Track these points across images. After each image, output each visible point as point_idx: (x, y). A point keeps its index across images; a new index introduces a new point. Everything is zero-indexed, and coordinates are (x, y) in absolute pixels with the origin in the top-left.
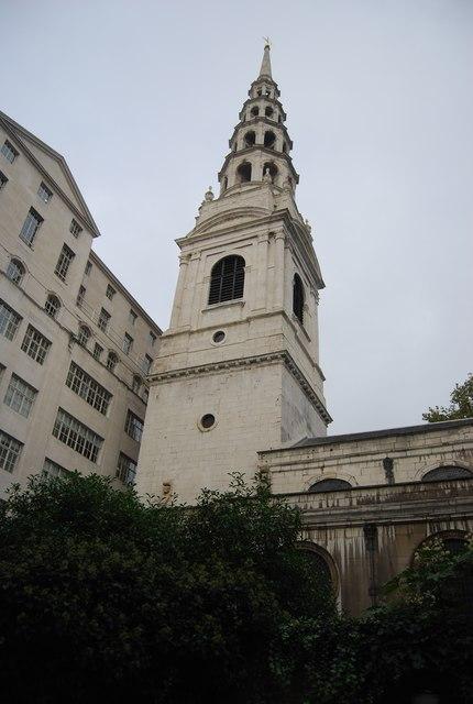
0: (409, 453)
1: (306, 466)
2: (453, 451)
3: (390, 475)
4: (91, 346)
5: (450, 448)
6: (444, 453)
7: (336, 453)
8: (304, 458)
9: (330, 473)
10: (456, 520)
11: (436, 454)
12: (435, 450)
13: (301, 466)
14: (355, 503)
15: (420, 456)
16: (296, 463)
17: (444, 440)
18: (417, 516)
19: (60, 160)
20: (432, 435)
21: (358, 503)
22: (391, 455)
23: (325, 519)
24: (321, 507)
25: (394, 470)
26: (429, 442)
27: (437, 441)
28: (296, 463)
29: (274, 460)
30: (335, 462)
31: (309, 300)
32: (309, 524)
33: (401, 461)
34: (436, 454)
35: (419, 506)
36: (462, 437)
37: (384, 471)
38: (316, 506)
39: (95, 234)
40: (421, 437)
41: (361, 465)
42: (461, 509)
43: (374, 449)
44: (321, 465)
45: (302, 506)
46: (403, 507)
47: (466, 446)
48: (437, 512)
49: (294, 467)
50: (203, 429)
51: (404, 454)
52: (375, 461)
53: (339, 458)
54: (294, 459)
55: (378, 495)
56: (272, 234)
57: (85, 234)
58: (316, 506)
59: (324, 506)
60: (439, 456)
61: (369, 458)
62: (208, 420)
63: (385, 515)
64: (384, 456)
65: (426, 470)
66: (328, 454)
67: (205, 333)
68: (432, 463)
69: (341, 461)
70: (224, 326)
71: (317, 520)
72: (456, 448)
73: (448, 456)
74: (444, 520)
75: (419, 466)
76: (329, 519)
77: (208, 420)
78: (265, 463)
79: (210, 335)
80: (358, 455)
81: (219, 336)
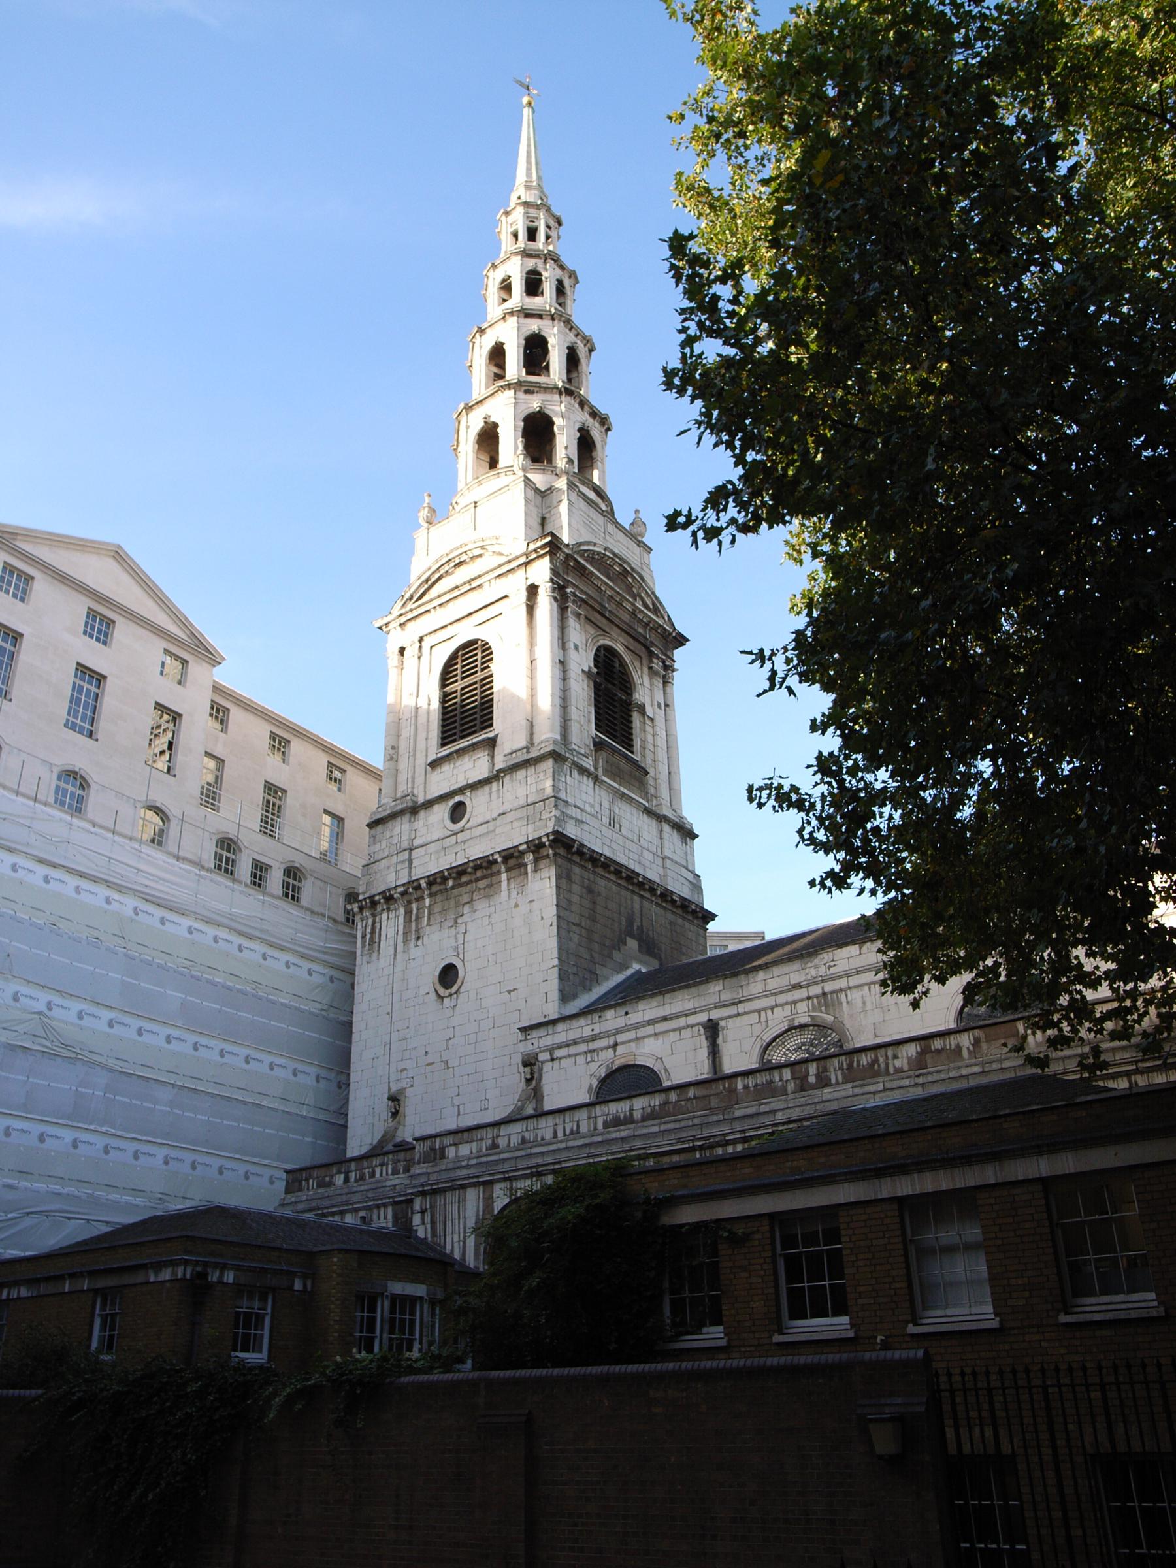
0: (741, 1008)
1: (592, 1046)
2: (809, 998)
3: (714, 1052)
4: (244, 869)
5: (801, 994)
6: (795, 1002)
7: (635, 1018)
8: (587, 1032)
9: (623, 1056)
10: (734, 1142)
11: (782, 1005)
12: (781, 999)
13: (583, 1048)
14: (600, 1126)
15: (759, 1011)
16: (575, 1043)
17: (795, 978)
18: (679, 1141)
19: (119, 555)
20: (776, 971)
21: (606, 1125)
22: (715, 1014)
23: (558, 1157)
24: (555, 1133)
25: (720, 1041)
26: (773, 984)
27: (784, 982)
28: (575, 1043)
29: (541, 1041)
30: (631, 1035)
31: (645, 691)
32: (538, 1166)
33: (731, 1022)
34: (782, 1005)
35: (683, 1124)
36: (822, 970)
37: (705, 1043)
38: (548, 1135)
39: (212, 658)
40: (761, 975)
41: (674, 1036)
42: (738, 1126)
43: (689, 1005)
44: (611, 1041)
45: (529, 1136)
46: (663, 1128)
47: (829, 987)
48: (708, 1132)
49: (573, 1050)
50: (442, 991)
51: (732, 1010)
52: (692, 1026)
53: (636, 1027)
54: (573, 1035)
55: (631, 1110)
56: (533, 590)
57: (197, 669)
58: (548, 1135)
59: (560, 1134)
60: (788, 1008)
61: (682, 1022)
62: (448, 975)
63: (637, 1144)
64: (703, 1017)
65: (768, 1037)
66: (620, 1022)
67: (436, 808)
68: (778, 1021)
69: (642, 1032)
70: (461, 791)
71: (548, 1159)
72: (815, 990)
73: (802, 1007)
74: (719, 1145)
75: (757, 1029)
76: (565, 1155)
77: (448, 975)
78: (530, 1047)
79: (441, 812)
80: (665, 1019)
81: (458, 812)
